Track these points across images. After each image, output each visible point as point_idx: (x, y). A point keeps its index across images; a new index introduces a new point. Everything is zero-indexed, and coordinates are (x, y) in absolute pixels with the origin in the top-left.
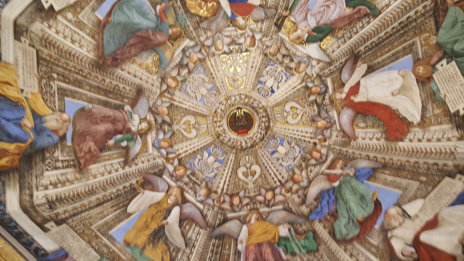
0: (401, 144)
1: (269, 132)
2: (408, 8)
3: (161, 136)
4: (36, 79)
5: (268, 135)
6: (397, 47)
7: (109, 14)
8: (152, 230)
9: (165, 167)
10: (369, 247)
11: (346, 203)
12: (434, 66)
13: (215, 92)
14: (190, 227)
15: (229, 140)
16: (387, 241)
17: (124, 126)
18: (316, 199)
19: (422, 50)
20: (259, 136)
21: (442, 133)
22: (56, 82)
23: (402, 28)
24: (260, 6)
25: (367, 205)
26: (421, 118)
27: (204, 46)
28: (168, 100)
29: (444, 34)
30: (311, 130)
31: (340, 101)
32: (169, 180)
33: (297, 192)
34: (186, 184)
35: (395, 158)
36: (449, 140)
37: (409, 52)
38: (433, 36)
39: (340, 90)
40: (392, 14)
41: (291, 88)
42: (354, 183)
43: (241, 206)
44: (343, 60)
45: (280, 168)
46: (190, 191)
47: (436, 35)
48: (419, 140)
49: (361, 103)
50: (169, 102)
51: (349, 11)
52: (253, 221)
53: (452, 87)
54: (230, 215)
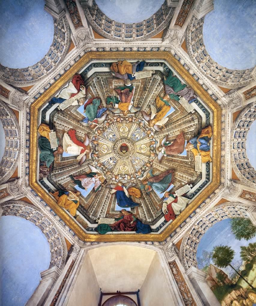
0: (72, 128)
1: (114, 143)
3: (154, 145)
4: (196, 161)
5: (115, 142)
7: (169, 186)
8: (161, 111)
9: (154, 134)
10: (92, 94)
11: (94, 111)
12: (57, 150)
13: (133, 161)
14: (148, 112)
15: (129, 142)
16: (86, 94)
17: (167, 149)
18: (103, 115)
20: (118, 143)
22: (189, 161)
23: (63, 168)
24: (112, 189)
25: (88, 108)
27: (135, 178)
28: (150, 159)
30: (99, 141)
32: (153, 129)
33: (109, 119)
34: (147, 127)
35: (74, 123)
36: (58, 123)
41: (104, 158)
42: (90, 118)
43: (129, 117)
44: (84, 164)
45: (113, 129)
46: (146, 125)
47: (54, 160)
48: (66, 127)
49: (81, 146)
50: (150, 158)
51: (80, 179)
52: (126, 111)
54: (134, 115)
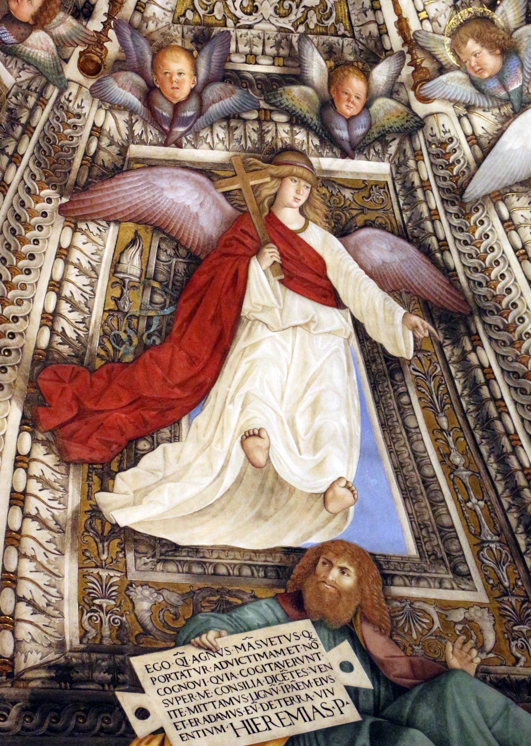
6: (461, 504)
19: (425, 601)
21: (41, 602)
26: (126, 528)
29: (480, 703)
31: (266, 192)
37: (428, 547)
38: (478, 660)
39: (322, 209)
53: (245, 686)
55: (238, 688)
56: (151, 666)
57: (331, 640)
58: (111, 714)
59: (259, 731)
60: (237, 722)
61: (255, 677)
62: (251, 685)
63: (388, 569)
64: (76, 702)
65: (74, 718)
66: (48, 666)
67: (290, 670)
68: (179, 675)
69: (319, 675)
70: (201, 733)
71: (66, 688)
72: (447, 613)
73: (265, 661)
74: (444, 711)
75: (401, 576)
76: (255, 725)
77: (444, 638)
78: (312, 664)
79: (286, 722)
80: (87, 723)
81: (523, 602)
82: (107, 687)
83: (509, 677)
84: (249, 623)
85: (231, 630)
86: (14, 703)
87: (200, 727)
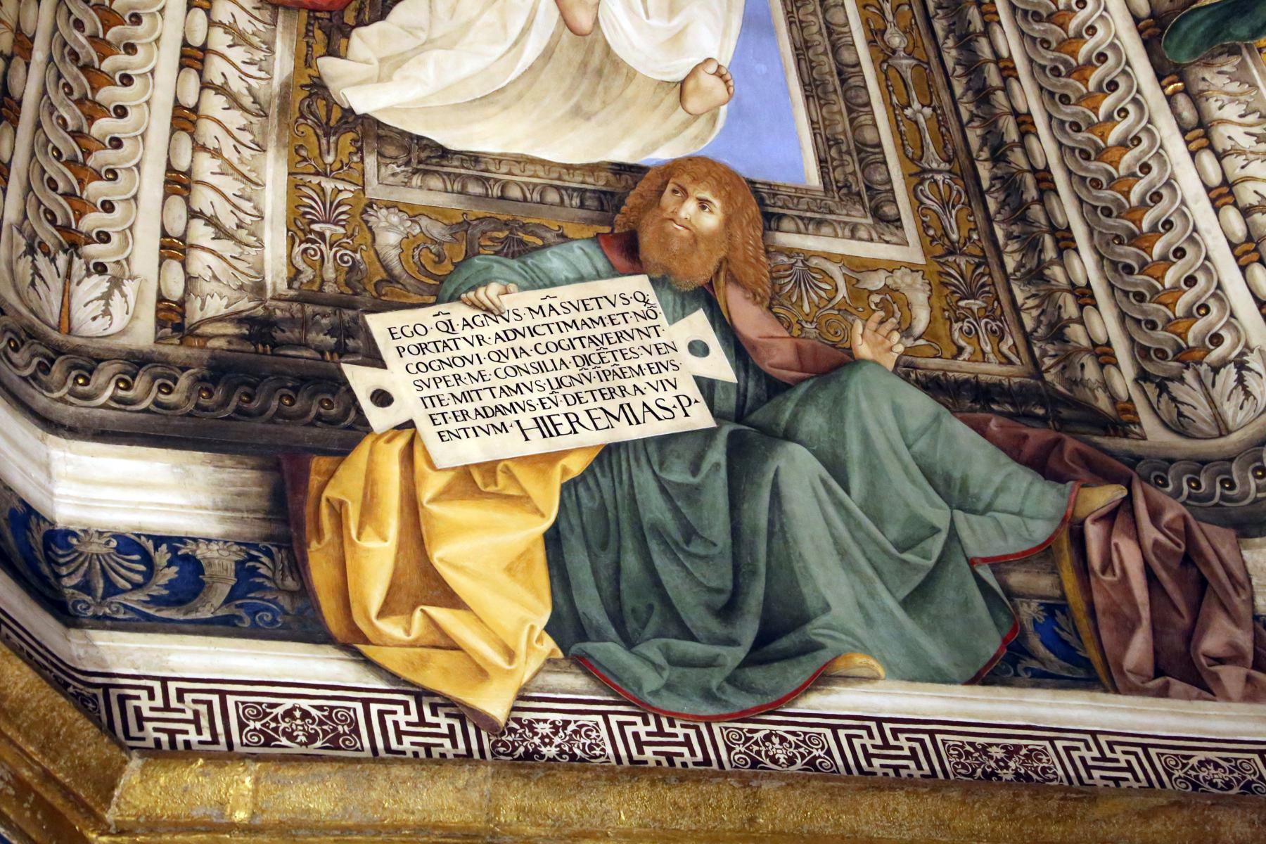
2: (1128, 253)
6: (895, 111)
19: (828, 257)
21: (229, 222)
23: (1010, 184)
26: (365, 117)
29: (897, 411)
37: (838, 174)
38: (900, 348)
40: (1127, 143)
47: (905, 369)
53: (541, 367)
55: (531, 370)
56: (398, 330)
57: (678, 308)
58: (334, 395)
59: (559, 434)
60: (526, 419)
61: (556, 357)
62: (550, 366)
63: (774, 206)
64: (280, 375)
65: (277, 396)
66: (238, 319)
67: (611, 348)
68: (440, 345)
69: (656, 358)
70: (470, 432)
71: (265, 353)
72: (858, 276)
73: (573, 333)
74: (842, 418)
75: (792, 218)
76: (554, 426)
77: (852, 314)
78: (647, 342)
79: (602, 423)
80: (295, 407)
81: (978, 266)
82: (328, 356)
83: (945, 374)
84: (552, 275)
85: (525, 283)
86: (184, 369)
87: (469, 423)
